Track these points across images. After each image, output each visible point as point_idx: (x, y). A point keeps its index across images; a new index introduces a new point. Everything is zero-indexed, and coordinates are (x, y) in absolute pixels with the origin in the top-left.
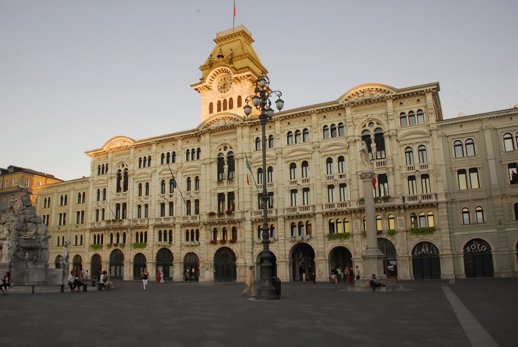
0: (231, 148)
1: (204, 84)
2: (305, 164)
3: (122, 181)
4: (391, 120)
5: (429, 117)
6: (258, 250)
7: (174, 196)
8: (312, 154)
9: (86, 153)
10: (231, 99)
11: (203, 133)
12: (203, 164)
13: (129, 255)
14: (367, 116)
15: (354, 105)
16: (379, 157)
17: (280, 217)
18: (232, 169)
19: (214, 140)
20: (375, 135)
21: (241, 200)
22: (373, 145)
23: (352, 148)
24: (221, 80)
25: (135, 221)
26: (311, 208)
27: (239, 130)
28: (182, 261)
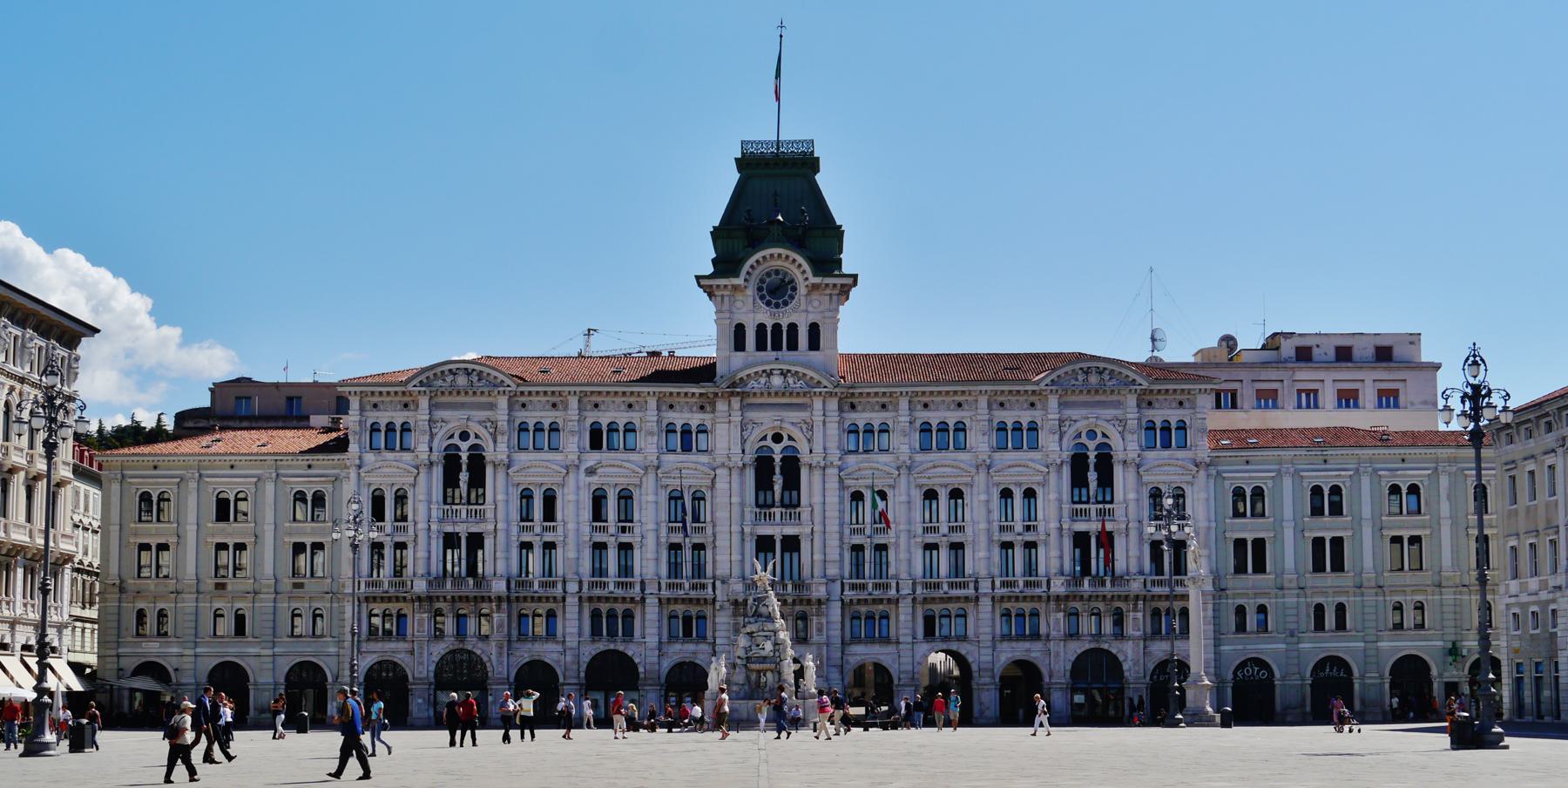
2: (956, 494)
3: (464, 477)
7: (637, 531)
10: (793, 328)
12: (723, 465)
16: (1100, 498)
18: (792, 482)
19: (752, 415)
22: (1092, 476)
23: (1053, 478)
24: (769, 274)
27: (818, 404)
28: (663, 680)
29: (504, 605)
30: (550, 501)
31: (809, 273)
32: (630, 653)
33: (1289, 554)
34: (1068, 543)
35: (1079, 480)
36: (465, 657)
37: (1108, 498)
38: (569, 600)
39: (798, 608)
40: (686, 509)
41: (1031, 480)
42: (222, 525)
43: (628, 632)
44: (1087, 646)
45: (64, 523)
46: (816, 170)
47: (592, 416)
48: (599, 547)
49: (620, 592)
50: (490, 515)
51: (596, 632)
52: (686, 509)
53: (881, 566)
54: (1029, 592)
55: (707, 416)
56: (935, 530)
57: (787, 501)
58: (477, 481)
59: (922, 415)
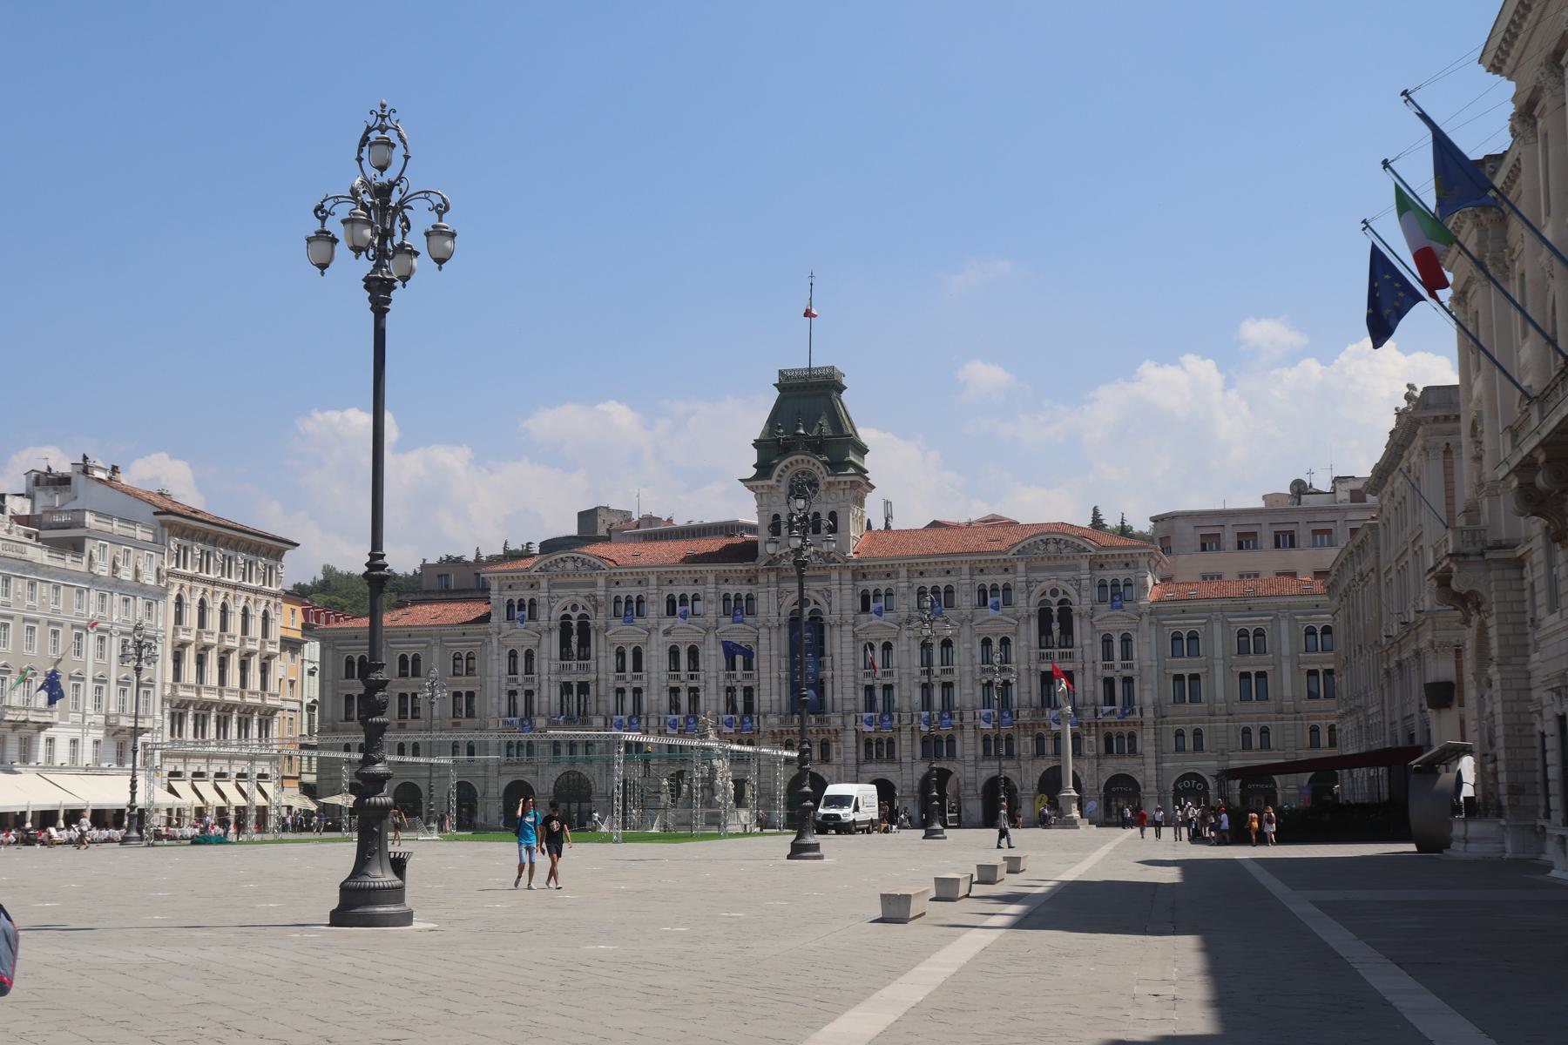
3: (575, 639)
10: (817, 515)
22: (1056, 626)
23: (1023, 628)
27: (835, 575)
30: (637, 654)
33: (1220, 686)
35: (1045, 630)
41: (1005, 630)
42: (403, 679)
45: (273, 686)
46: (841, 388)
48: (674, 691)
50: (593, 667)
59: (919, 582)
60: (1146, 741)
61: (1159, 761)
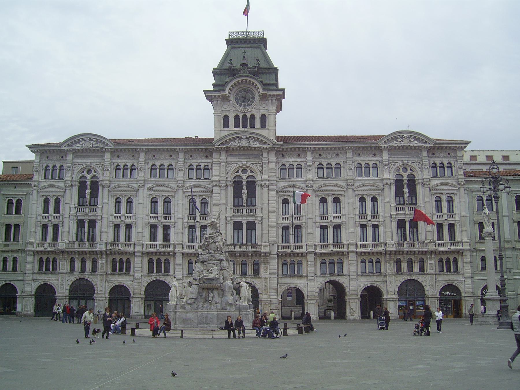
0: (251, 171)
1: (223, 93)
2: (337, 200)
3: (88, 191)
4: (426, 169)
5: (458, 171)
6: (283, 287)
7: (172, 218)
8: (345, 191)
9: (27, 146)
10: (253, 117)
11: (219, 151)
12: (216, 185)
13: (103, 286)
14: (403, 161)
15: (392, 150)
16: (410, 202)
17: (310, 253)
18: (252, 194)
20: (408, 181)
21: (265, 231)
22: (406, 190)
23: (387, 190)
25: (112, 245)
26: (345, 246)
27: (265, 155)
29: (104, 256)
31: (261, 89)
32: (167, 282)
34: (395, 225)
35: (399, 193)
36: (85, 282)
37: (414, 202)
38: (136, 254)
39: (254, 259)
40: (198, 205)
43: (167, 271)
44: (407, 278)
47: (152, 161)
48: (153, 228)
49: (162, 249)
51: (150, 270)
52: (198, 205)
53: (299, 238)
54: (375, 249)
55: (209, 161)
56: (326, 218)
57: (249, 204)
58: (94, 194)
60: (465, 264)
61: (473, 275)
